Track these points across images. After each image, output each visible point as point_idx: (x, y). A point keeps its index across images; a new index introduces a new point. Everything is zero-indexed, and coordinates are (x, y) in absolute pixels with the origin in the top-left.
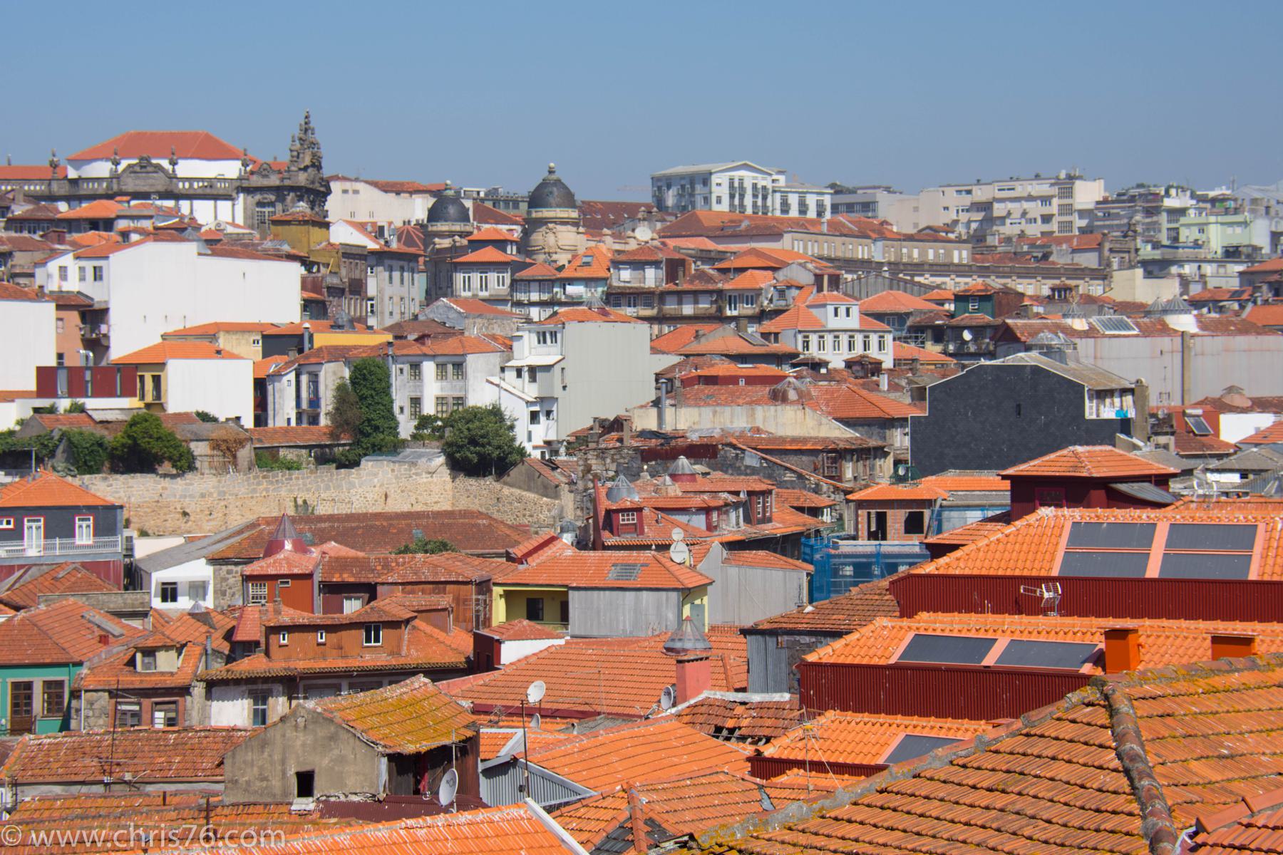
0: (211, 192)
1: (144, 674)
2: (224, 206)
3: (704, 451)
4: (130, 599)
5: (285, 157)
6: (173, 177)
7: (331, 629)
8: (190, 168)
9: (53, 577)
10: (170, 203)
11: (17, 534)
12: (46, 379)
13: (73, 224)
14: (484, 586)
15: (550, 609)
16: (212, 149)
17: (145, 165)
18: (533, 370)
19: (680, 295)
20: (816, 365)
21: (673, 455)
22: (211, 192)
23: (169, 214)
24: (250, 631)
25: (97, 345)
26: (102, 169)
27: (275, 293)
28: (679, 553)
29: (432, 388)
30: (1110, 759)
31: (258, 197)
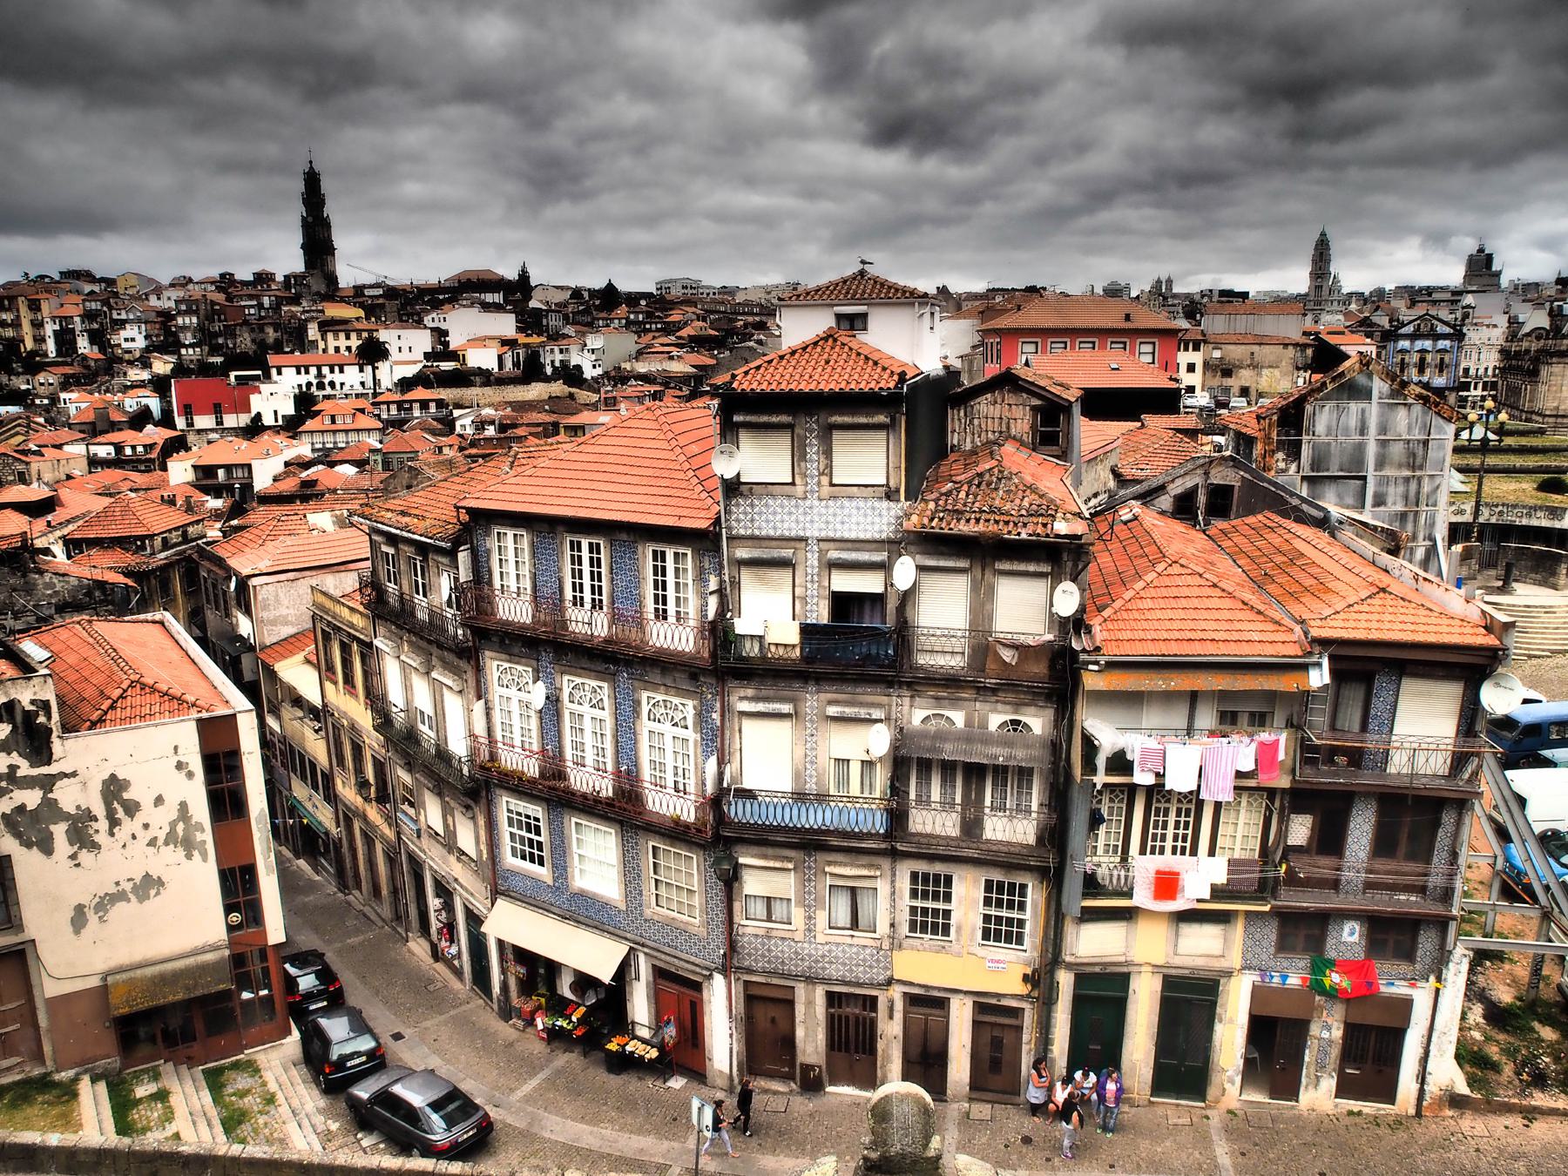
11: (411, 409)
12: (427, 356)
25: (446, 344)
29: (558, 357)
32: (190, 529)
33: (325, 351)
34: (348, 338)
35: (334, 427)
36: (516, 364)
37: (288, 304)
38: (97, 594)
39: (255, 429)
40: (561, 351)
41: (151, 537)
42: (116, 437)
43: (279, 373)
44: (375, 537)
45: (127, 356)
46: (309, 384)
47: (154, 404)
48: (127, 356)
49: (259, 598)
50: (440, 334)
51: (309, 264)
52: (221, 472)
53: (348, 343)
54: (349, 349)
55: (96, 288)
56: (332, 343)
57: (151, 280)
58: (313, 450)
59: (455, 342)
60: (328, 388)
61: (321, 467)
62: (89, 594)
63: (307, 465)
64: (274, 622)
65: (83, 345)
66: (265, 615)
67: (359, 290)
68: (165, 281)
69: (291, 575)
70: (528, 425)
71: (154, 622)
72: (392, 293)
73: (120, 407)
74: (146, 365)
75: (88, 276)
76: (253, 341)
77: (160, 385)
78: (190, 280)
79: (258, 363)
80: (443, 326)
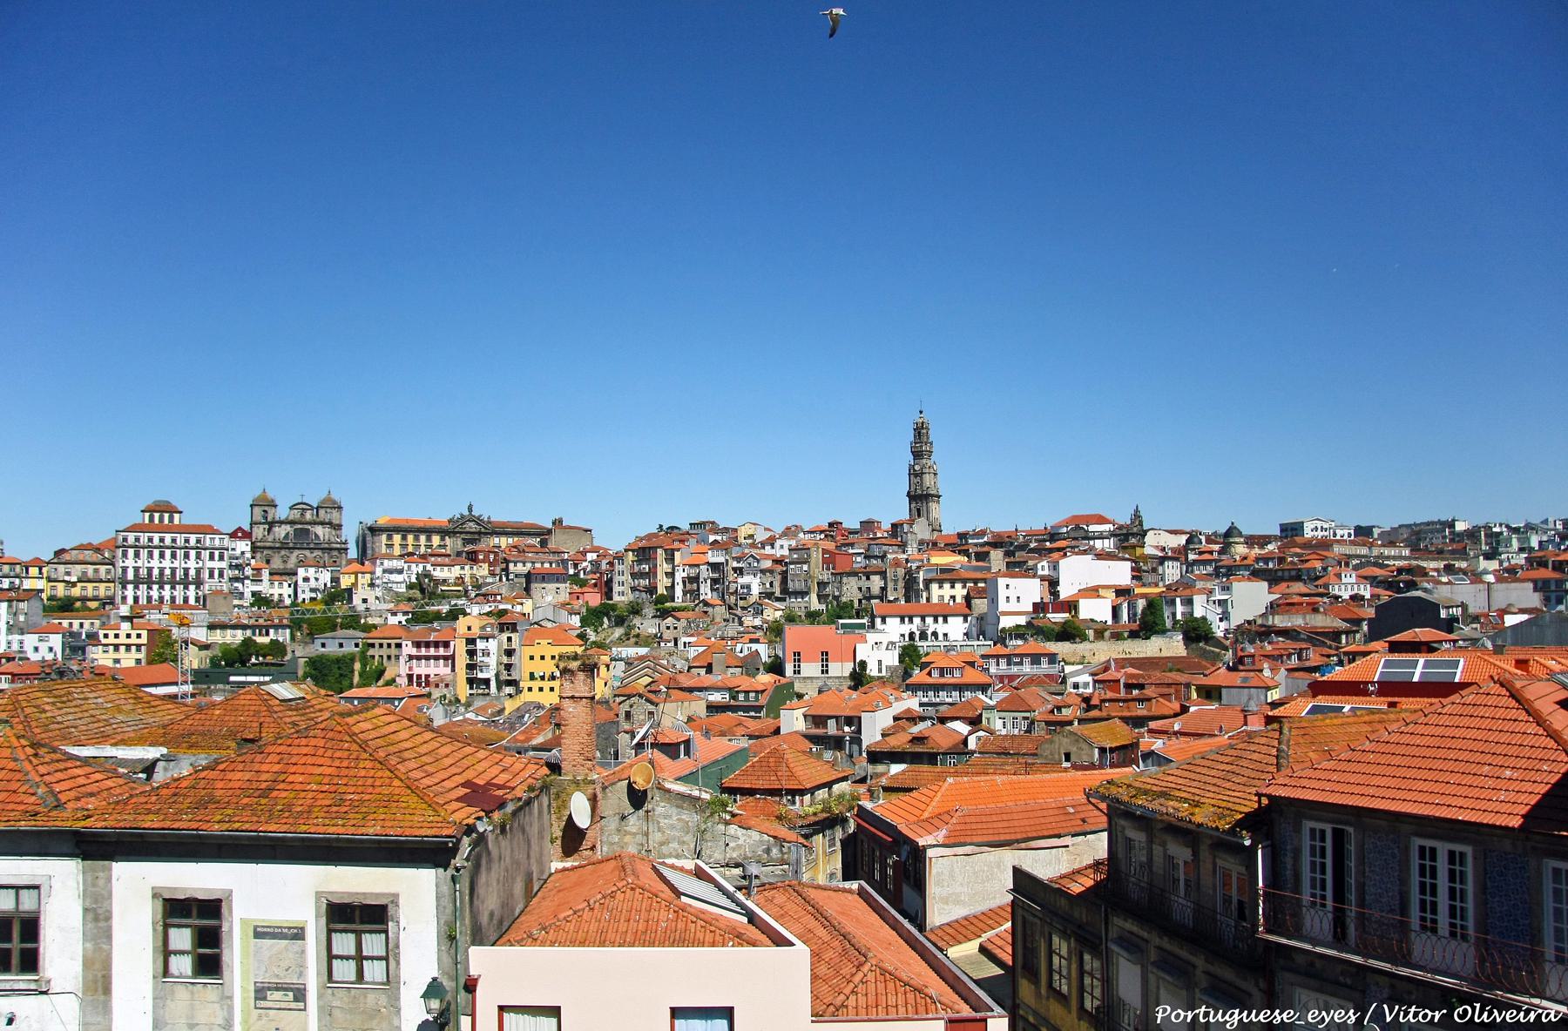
1: (1057, 716)
4: (1059, 688)
7: (1125, 701)
8: (1092, 528)
9: (1032, 680)
11: (1021, 663)
13: (1051, 550)
14: (1188, 686)
15: (1214, 694)
16: (1101, 520)
17: (1077, 528)
20: (1337, 597)
24: (1095, 701)
25: (1055, 594)
28: (1267, 673)
30: (1274, 752)
33: (928, 599)
35: (942, 681)
36: (1132, 617)
38: (775, 852)
39: (859, 678)
43: (884, 621)
44: (1122, 822)
45: (741, 603)
46: (912, 635)
49: (934, 871)
50: (1053, 583)
52: (832, 723)
53: (953, 592)
54: (953, 597)
55: (719, 538)
58: (921, 705)
59: (1065, 592)
61: (929, 723)
62: (768, 851)
63: (914, 719)
64: (945, 900)
65: (706, 592)
67: (962, 536)
69: (968, 849)
74: (759, 612)
79: (865, 613)
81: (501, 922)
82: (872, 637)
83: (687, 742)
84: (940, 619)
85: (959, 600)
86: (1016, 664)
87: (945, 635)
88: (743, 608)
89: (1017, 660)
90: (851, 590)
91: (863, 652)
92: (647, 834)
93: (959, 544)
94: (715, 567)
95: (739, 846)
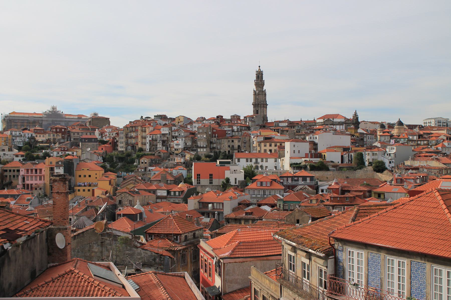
0: (340, 124)
2: (341, 126)
3: (417, 169)
5: (352, 118)
6: (333, 121)
8: (336, 120)
10: (332, 126)
11: (298, 180)
12: (307, 156)
14: (370, 192)
15: (382, 196)
18: (390, 154)
19: (421, 141)
21: (408, 169)
22: (340, 124)
23: (332, 127)
25: (316, 149)
26: (322, 121)
27: (346, 141)
31: (347, 125)
32: (197, 232)
34: (270, 145)
36: (350, 161)
37: (245, 130)
39: (226, 185)
40: (373, 154)
41: (181, 234)
42: (170, 187)
43: (239, 161)
46: (251, 166)
47: (184, 172)
48: (176, 152)
49: (226, 269)
50: (314, 145)
51: (256, 112)
52: (210, 205)
53: (270, 148)
54: (271, 151)
55: (167, 123)
56: (263, 148)
57: (189, 119)
59: (320, 150)
60: (260, 169)
62: (154, 260)
63: (248, 205)
65: (160, 146)
66: (227, 277)
68: (194, 119)
69: (241, 260)
70: (356, 191)
71: (180, 276)
72: (292, 124)
73: (171, 174)
75: (163, 117)
76: (229, 146)
77: (188, 165)
78: (204, 119)
80: (316, 141)
81: (16, 288)
82: (232, 168)
83: (141, 214)
84: (264, 160)
85: (273, 151)
86: (295, 180)
87: (266, 167)
88: (177, 154)
89: (296, 179)
90: (224, 146)
91: (228, 174)
92: (102, 252)
93: (276, 126)
94: (164, 135)
95: (142, 258)
